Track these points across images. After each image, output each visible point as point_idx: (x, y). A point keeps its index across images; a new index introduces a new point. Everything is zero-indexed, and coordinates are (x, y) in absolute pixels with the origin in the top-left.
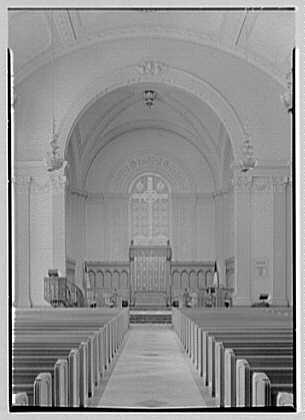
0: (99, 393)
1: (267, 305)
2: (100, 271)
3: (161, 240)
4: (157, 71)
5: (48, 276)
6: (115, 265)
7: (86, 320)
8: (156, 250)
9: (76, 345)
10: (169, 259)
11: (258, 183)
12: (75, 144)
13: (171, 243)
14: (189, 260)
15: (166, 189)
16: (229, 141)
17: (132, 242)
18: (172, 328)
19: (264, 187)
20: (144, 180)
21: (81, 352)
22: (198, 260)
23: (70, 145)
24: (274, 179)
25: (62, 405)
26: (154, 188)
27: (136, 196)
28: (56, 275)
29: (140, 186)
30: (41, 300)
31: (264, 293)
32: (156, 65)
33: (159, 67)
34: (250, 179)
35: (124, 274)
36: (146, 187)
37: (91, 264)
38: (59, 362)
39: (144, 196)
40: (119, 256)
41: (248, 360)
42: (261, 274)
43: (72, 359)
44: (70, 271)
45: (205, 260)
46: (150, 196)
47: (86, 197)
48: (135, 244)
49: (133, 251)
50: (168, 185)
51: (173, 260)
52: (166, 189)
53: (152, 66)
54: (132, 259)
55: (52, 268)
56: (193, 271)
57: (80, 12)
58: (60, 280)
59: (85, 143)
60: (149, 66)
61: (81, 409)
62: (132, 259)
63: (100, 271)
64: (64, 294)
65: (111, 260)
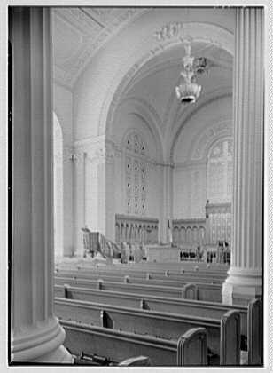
6: (194, 221)
17: (208, 202)
20: (221, 145)
27: (212, 161)
35: (182, 230)
36: (222, 149)
37: (173, 223)
40: (202, 216)
47: (173, 167)
48: (210, 203)
50: (229, 138)
53: (168, 30)
54: (207, 216)
56: (195, 227)
58: (91, 234)
62: (207, 216)
63: (183, 228)
65: (192, 217)
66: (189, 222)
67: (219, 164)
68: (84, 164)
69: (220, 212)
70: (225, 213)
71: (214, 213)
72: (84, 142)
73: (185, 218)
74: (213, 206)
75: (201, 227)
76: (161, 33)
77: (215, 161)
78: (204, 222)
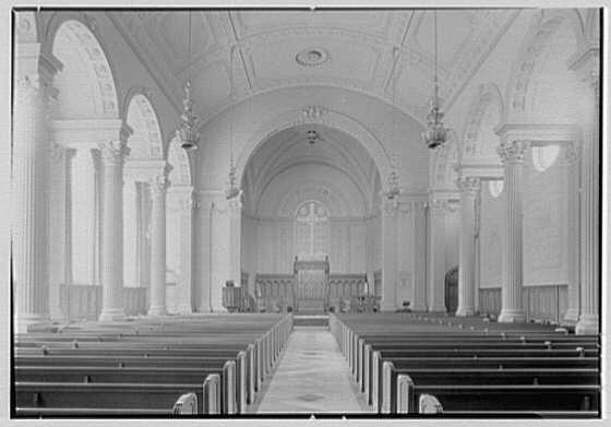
0: (259, 401)
1: (409, 311)
2: (269, 282)
3: (320, 256)
4: (318, 114)
5: (225, 285)
7: (257, 324)
8: (316, 264)
9: (244, 348)
10: (327, 272)
11: (403, 208)
12: (249, 174)
13: (329, 259)
14: (344, 272)
15: (325, 214)
16: (378, 174)
18: (329, 330)
19: (406, 212)
21: (248, 354)
22: (354, 272)
23: (245, 177)
24: (416, 205)
25: (211, 413)
26: (316, 212)
27: (299, 219)
28: (232, 285)
29: (303, 210)
30: (216, 304)
31: (406, 300)
32: (318, 109)
33: (321, 113)
34: (395, 205)
36: (309, 212)
37: (262, 276)
38: (228, 363)
39: (308, 219)
40: (285, 269)
41: (393, 362)
42: (404, 284)
43: (240, 360)
44: (244, 282)
45: (357, 272)
46: (312, 219)
48: (300, 259)
49: (298, 265)
51: (331, 271)
52: (325, 214)
53: (315, 111)
54: (296, 272)
55: (229, 279)
57: (242, 12)
58: (236, 289)
59: (259, 175)
60: (312, 111)
61: (238, 416)
62: (296, 272)
63: (269, 282)
64: (237, 299)
65: (278, 272)
66: (274, 276)
67: (306, 224)
68: (211, 215)
69: (309, 269)
70: (315, 268)
71: (303, 268)
72: (211, 192)
73: (271, 272)
74: (301, 263)
75: (289, 282)
76: (308, 112)
77: (303, 220)
78: (293, 277)
